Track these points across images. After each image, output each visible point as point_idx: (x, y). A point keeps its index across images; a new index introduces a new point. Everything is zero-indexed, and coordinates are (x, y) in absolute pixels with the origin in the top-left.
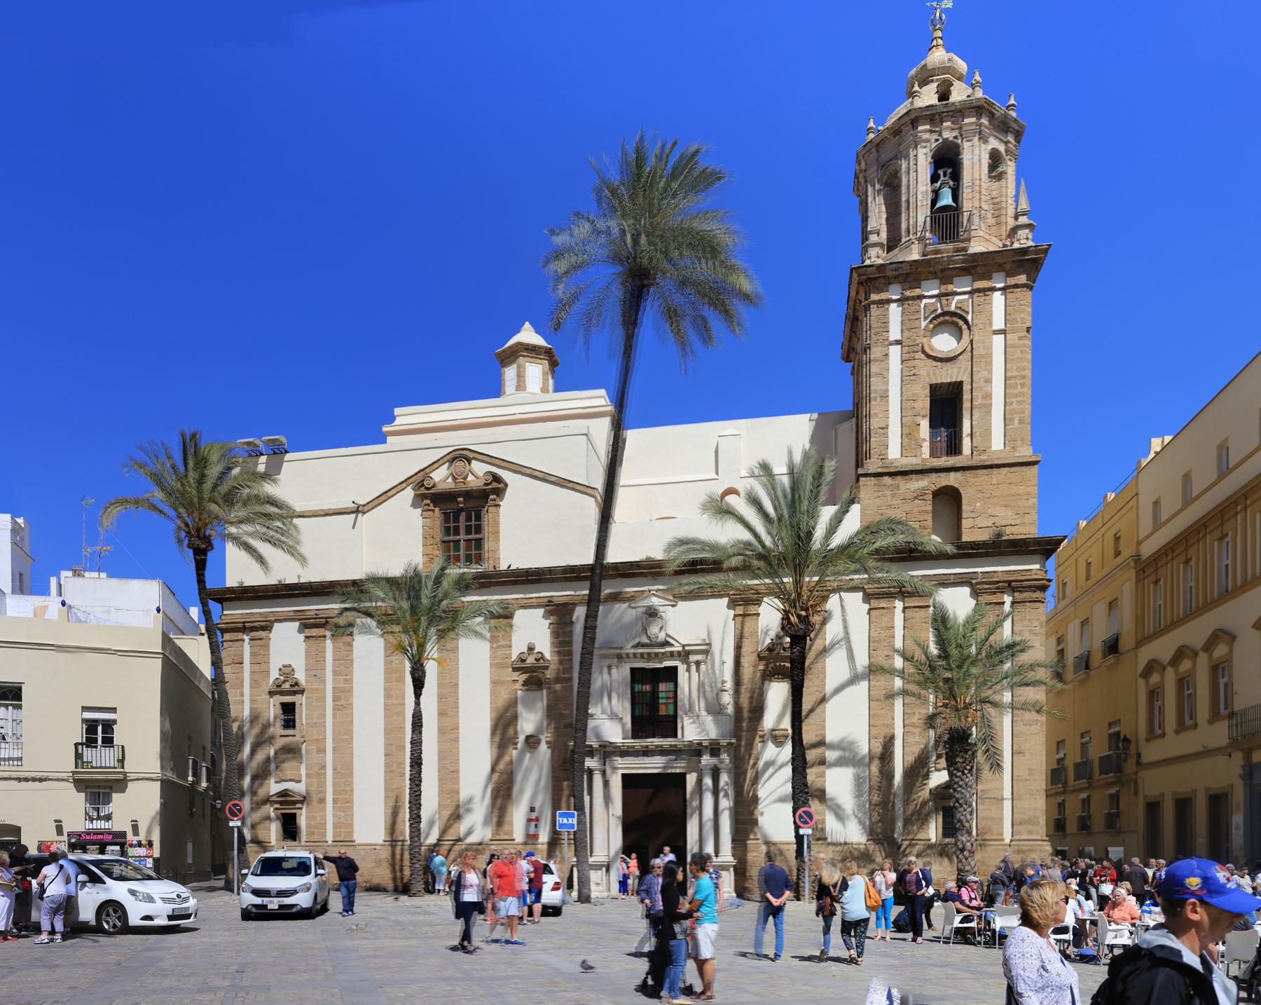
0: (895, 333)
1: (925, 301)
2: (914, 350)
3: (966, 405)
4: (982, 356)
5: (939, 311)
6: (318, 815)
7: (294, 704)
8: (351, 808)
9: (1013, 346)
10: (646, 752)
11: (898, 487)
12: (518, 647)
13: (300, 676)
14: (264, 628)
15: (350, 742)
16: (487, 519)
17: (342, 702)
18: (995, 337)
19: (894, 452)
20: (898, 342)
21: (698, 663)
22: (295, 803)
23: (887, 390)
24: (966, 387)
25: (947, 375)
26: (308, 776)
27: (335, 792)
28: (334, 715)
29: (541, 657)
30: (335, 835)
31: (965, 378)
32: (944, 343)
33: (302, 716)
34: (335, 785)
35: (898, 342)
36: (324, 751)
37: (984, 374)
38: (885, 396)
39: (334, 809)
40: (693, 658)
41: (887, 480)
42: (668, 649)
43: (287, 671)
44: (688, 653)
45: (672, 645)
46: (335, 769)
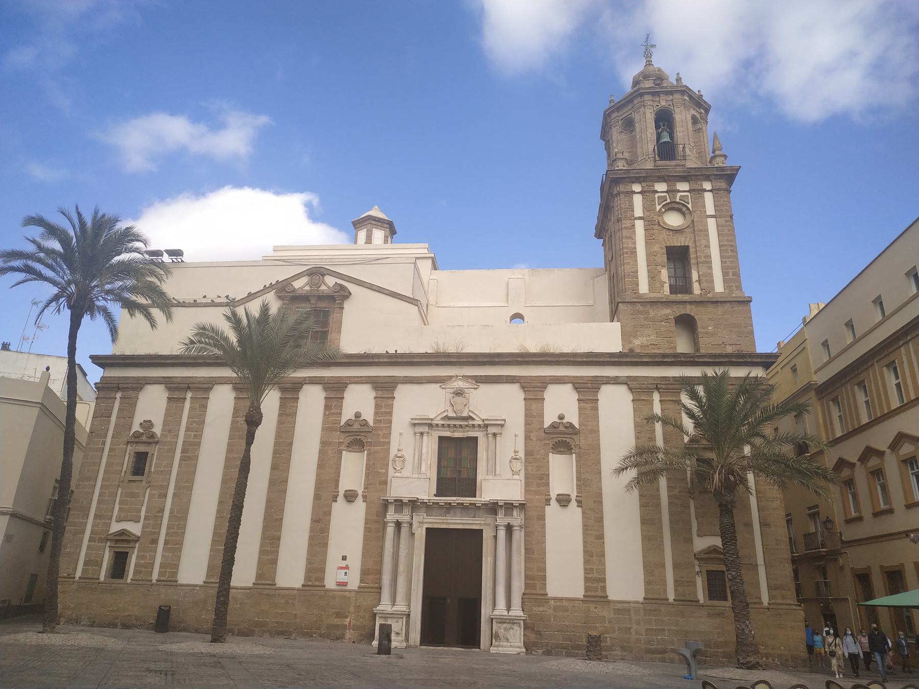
0: (638, 211)
1: (657, 195)
2: (653, 224)
3: (693, 261)
4: (701, 231)
5: (668, 201)
6: (148, 554)
7: (147, 453)
8: (180, 550)
9: (721, 226)
10: (449, 508)
11: (648, 313)
12: (347, 414)
13: (157, 430)
14: (134, 389)
15: (190, 489)
16: (333, 317)
17: (189, 454)
18: (709, 220)
19: (644, 288)
20: (640, 218)
21: (495, 435)
22: (128, 541)
23: (635, 248)
24: (692, 250)
25: (679, 241)
26: (146, 518)
27: (167, 534)
28: (180, 465)
29: (365, 423)
30: (161, 574)
31: (691, 244)
32: (674, 220)
33: (153, 465)
34: (169, 527)
35: (640, 218)
36: (165, 496)
37: (703, 242)
38: (634, 252)
39: (164, 550)
40: (491, 430)
41: (639, 307)
42: (471, 422)
43: (147, 425)
44: (486, 426)
45: (473, 419)
46: (171, 512)
